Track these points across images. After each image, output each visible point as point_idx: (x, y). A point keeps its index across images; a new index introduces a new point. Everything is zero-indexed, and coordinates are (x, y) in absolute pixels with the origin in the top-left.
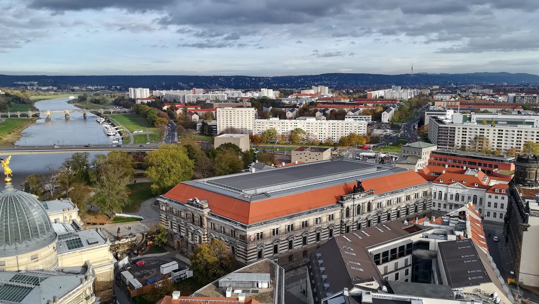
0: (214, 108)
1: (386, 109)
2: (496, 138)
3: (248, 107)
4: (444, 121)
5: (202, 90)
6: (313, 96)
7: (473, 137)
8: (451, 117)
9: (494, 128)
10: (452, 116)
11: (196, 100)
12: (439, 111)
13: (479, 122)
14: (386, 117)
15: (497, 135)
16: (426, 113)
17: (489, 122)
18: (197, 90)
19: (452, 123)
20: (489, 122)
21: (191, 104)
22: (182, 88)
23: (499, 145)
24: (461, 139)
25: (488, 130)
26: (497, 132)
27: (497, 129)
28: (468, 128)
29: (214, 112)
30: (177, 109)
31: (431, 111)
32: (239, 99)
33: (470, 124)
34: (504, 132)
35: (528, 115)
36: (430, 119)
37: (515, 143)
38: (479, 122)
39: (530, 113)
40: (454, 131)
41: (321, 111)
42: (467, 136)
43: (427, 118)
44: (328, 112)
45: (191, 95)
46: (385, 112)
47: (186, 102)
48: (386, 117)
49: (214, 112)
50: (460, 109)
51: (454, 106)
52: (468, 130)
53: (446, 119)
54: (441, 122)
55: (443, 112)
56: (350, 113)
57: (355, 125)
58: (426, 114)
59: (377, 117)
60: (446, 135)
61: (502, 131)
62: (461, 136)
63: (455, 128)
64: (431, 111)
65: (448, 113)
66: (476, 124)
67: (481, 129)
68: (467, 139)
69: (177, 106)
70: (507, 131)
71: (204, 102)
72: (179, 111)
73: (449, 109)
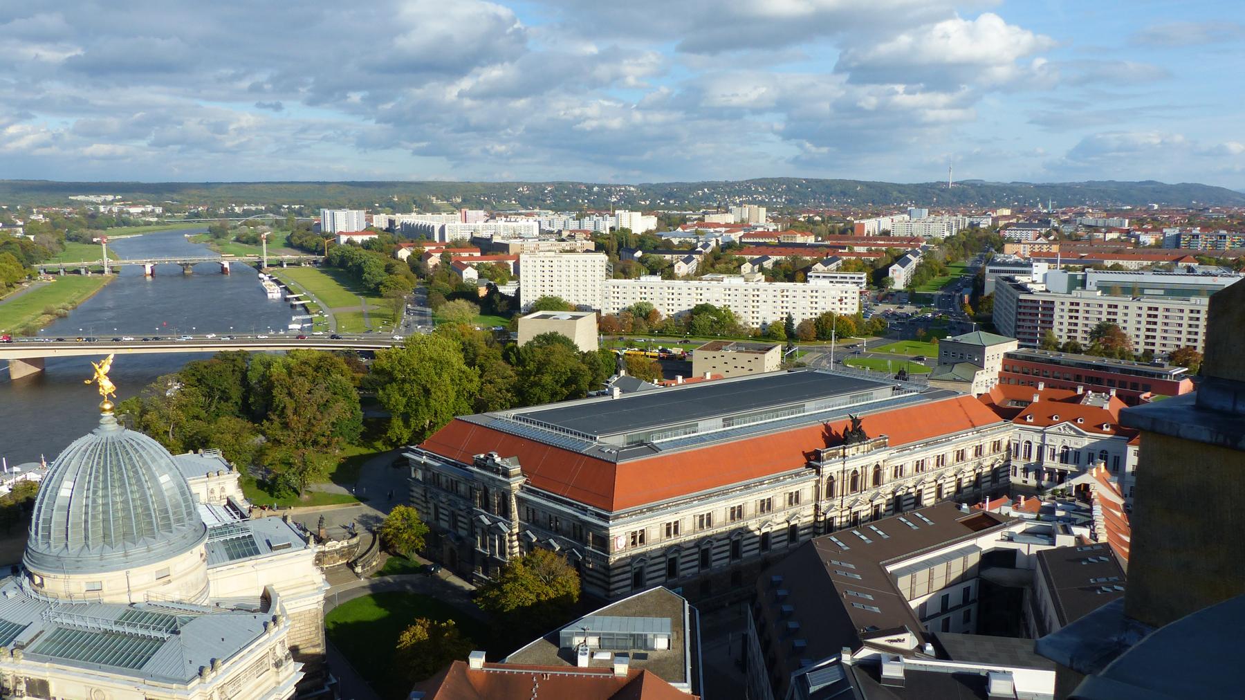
0: (512, 252)
1: (901, 259)
2: (1143, 326)
3: (588, 251)
4: (1029, 286)
5: (481, 213)
6: (732, 227)
7: (1093, 323)
8: (1040, 279)
9: (1140, 304)
10: (1045, 275)
11: (468, 237)
12: (1017, 264)
13: (1106, 289)
14: (899, 277)
15: (1144, 319)
16: (988, 269)
17: (1127, 290)
18: (471, 213)
19: (1047, 291)
20: (1127, 290)
21: (458, 244)
22: (436, 210)
23: (1150, 340)
24: (1065, 327)
25: (1126, 308)
26: (1145, 312)
27: (1145, 306)
28: (1082, 302)
29: (511, 263)
30: (429, 255)
31: (999, 264)
32: (565, 234)
33: (1085, 294)
34: (1160, 313)
35: (1211, 275)
36: (997, 283)
37: (1184, 336)
38: (1106, 289)
39: (1214, 271)
40: (1052, 309)
41: (753, 262)
42: (1080, 321)
43: (990, 282)
44: (768, 264)
45: (459, 223)
46: (896, 266)
47: (447, 240)
48: (899, 277)
49: (511, 263)
50: (1062, 262)
51: (1048, 254)
52: (1081, 308)
53: (1034, 282)
54: (1022, 288)
55: (1025, 266)
56: (819, 266)
57: (831, 294)
58: (987, 271)
59: (879, 277)
60: (1029, 319)
61: (1156, 309)
62: (1066, 320)
63: (1053, 302)
64: (999, 264)
65: (1035, 270)
66: (1099, 293)
67: (1110, 306)
68: (1080, 328)
69: (427, 249)
70: (1167, 310)
71: (490, 240)
72: (435, 260)
73: (1039, 261)
